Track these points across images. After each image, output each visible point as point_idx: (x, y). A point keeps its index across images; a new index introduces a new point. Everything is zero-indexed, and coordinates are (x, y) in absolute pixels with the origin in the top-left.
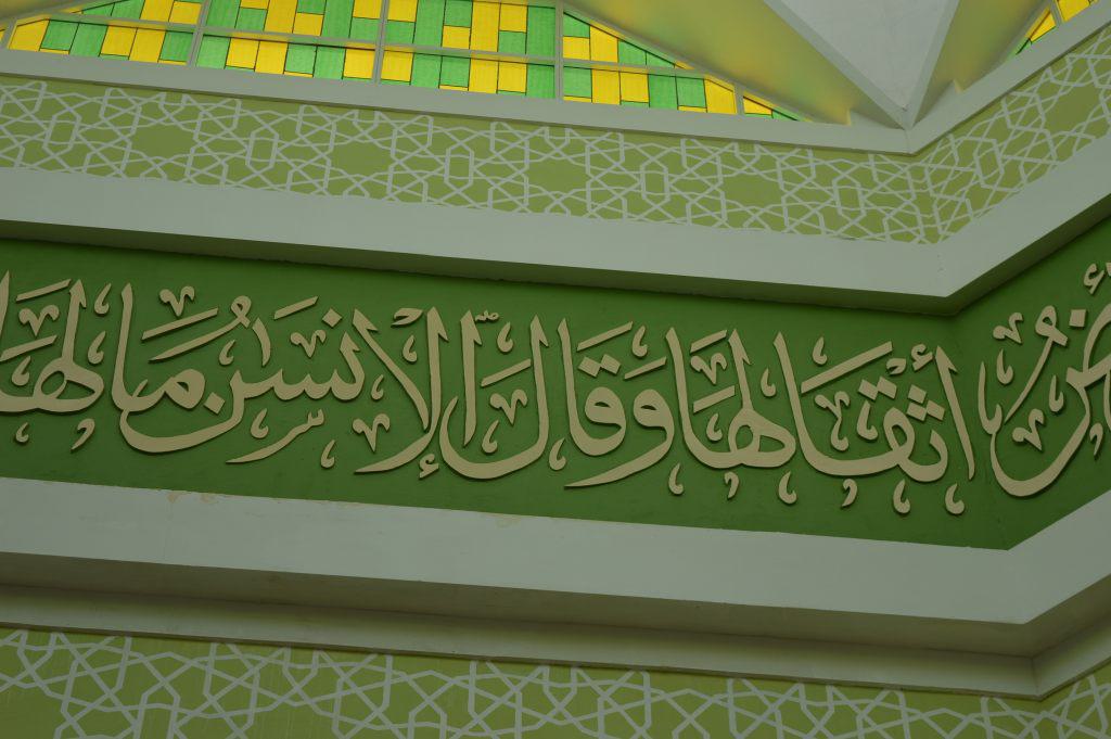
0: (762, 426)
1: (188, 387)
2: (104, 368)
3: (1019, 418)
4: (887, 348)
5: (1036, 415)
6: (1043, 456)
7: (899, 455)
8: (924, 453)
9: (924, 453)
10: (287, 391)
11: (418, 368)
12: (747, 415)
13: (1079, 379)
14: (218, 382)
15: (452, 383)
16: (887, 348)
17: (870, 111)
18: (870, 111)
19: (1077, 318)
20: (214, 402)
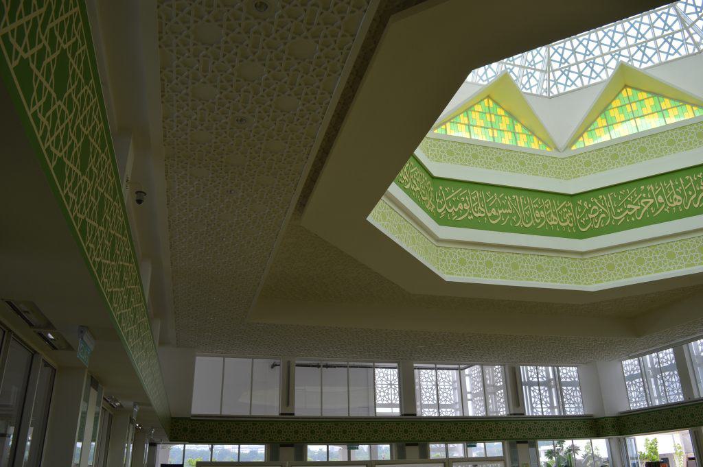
0: (555, 218)
1: (494, 211)
2: (484, 208)
3: (581, 218)
4: (565, 203)
5: (584, 219)
6: (584, 226)
7: (568, 222)
8: (571, 222)
9: (571, 222)
10: (504, 212)
11: (516, 207)
12: (552, 215)
13: (591, 216)
14: (497, 211)
15: (522, 211)
16: (565, 203)
17: (557, 149)
18: (557, 149)
19: (590, 206)
20: (497, 214)
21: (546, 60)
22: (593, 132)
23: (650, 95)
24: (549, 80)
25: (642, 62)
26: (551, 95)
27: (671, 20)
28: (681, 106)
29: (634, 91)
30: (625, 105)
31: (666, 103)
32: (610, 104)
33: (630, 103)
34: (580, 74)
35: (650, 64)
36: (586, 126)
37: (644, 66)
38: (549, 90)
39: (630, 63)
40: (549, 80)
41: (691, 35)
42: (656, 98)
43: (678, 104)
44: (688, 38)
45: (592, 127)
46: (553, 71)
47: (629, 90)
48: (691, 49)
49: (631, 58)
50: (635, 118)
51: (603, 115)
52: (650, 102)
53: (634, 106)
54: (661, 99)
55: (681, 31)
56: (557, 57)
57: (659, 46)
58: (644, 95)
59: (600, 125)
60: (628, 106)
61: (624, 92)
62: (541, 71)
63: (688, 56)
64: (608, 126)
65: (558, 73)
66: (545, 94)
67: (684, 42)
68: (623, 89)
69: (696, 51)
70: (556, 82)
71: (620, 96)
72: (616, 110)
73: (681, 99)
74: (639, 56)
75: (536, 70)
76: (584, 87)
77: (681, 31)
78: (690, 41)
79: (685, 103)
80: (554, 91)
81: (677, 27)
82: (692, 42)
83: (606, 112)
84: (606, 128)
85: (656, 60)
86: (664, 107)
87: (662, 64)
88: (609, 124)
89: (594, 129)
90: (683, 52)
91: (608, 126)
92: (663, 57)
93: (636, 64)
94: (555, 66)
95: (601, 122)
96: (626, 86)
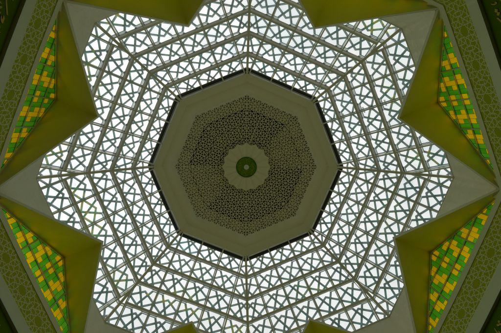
41: (378, 305)
44: (376, 308)
57: (351, 317)
78: (378, 310)
90: (374, 320)
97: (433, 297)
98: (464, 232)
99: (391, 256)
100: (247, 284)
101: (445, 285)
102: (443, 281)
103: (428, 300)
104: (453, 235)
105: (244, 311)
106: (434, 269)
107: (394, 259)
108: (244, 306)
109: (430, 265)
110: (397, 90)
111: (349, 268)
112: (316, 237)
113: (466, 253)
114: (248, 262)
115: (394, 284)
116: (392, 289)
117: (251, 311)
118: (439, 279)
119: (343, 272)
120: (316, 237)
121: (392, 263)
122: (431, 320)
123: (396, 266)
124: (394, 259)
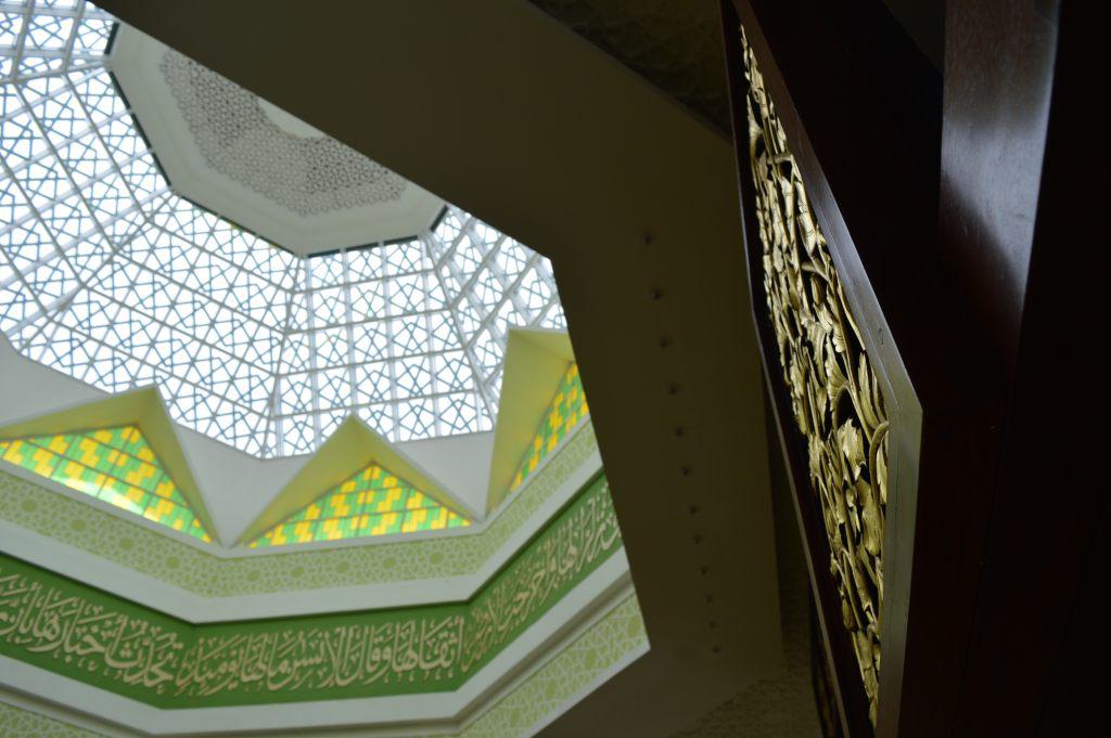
21: (62, 300)
22: (32, 449)
23: (156, 462)
24: (40, 330)
25: (183, 415)
26: (25, 352)
27: (259, 393)
28: (181, 505)
29: (142, 442)
30: (113, 448)
31: (167, 489)
32: (95, 429)
33: (122, 452)
34: (91, 362)
35: (191, 426)
36: (31, 434)
37: (181, 421)
38: (28, 344)
39: (168, 403)
40: (40, 330)
42: (160, 472)
43: (180, 500)
45: (38, 441)
46: (59, 324)
47: (137, 434)
48: (253, 449)
49: (175, 398)
50: (109, 475)
51: (69, 438)
52: (146, 473)
53: (124, 458)
54: (165, 478)
55: (261, 415)
56: (81, 311)
58: (147, 454)
59: (52, 448)
60: (113, 455)
61: (126, 432)
62: (43, 310)
63: (243, 453)
64: (62, 457)
65: (63, 334)
66: (17, 345)
67: (253, 434)
68: (128, 425)
69: (259, 455)
70: (49, 343)
71: (120, 431)
72: (95, 445)
73: (190, 499)
74: (186, 404)
75: (36, 299)
76: (81, 382)
77: (261, 415)
79: (190, 506)
80: (35, 354)
81: (259, 406)
82: (261, 443)
83: (78, 438)
84: (56, 459)
85: (202, 427)
86: (159, 492)
87: (204, 436)
88: (69, 454)
89: (38, 446)
90: (241, 444)
91: (62, 457)
92: (213, 432)
93: (174, 413)
94: (69, 319)
95: (59, 444)
96: (136, 425)
97: (313, 512)
98: (416, 500)
99: (345, 407)
100: (140, 228)
101: (333, 518)
102: (337, 514)
103: (305, 508)
104: (408, 485)
105: (95, 262)
106: (349, 487)
107: (341, 412)
108: (103, 254)
109: (354, 475)
110: (545, 309)
111: (289, 355)
112: (297, 269)
113: (384, 527)
114: (175, 198)
115: (309, 434)
116: (297, 441)
117: (108, 269)
118: (338, 503)
119: (277, 350)
120: (297, 269)
121: (335, 413)
122: (280, 530)
123: (334, 420)
124: (341, 412)
